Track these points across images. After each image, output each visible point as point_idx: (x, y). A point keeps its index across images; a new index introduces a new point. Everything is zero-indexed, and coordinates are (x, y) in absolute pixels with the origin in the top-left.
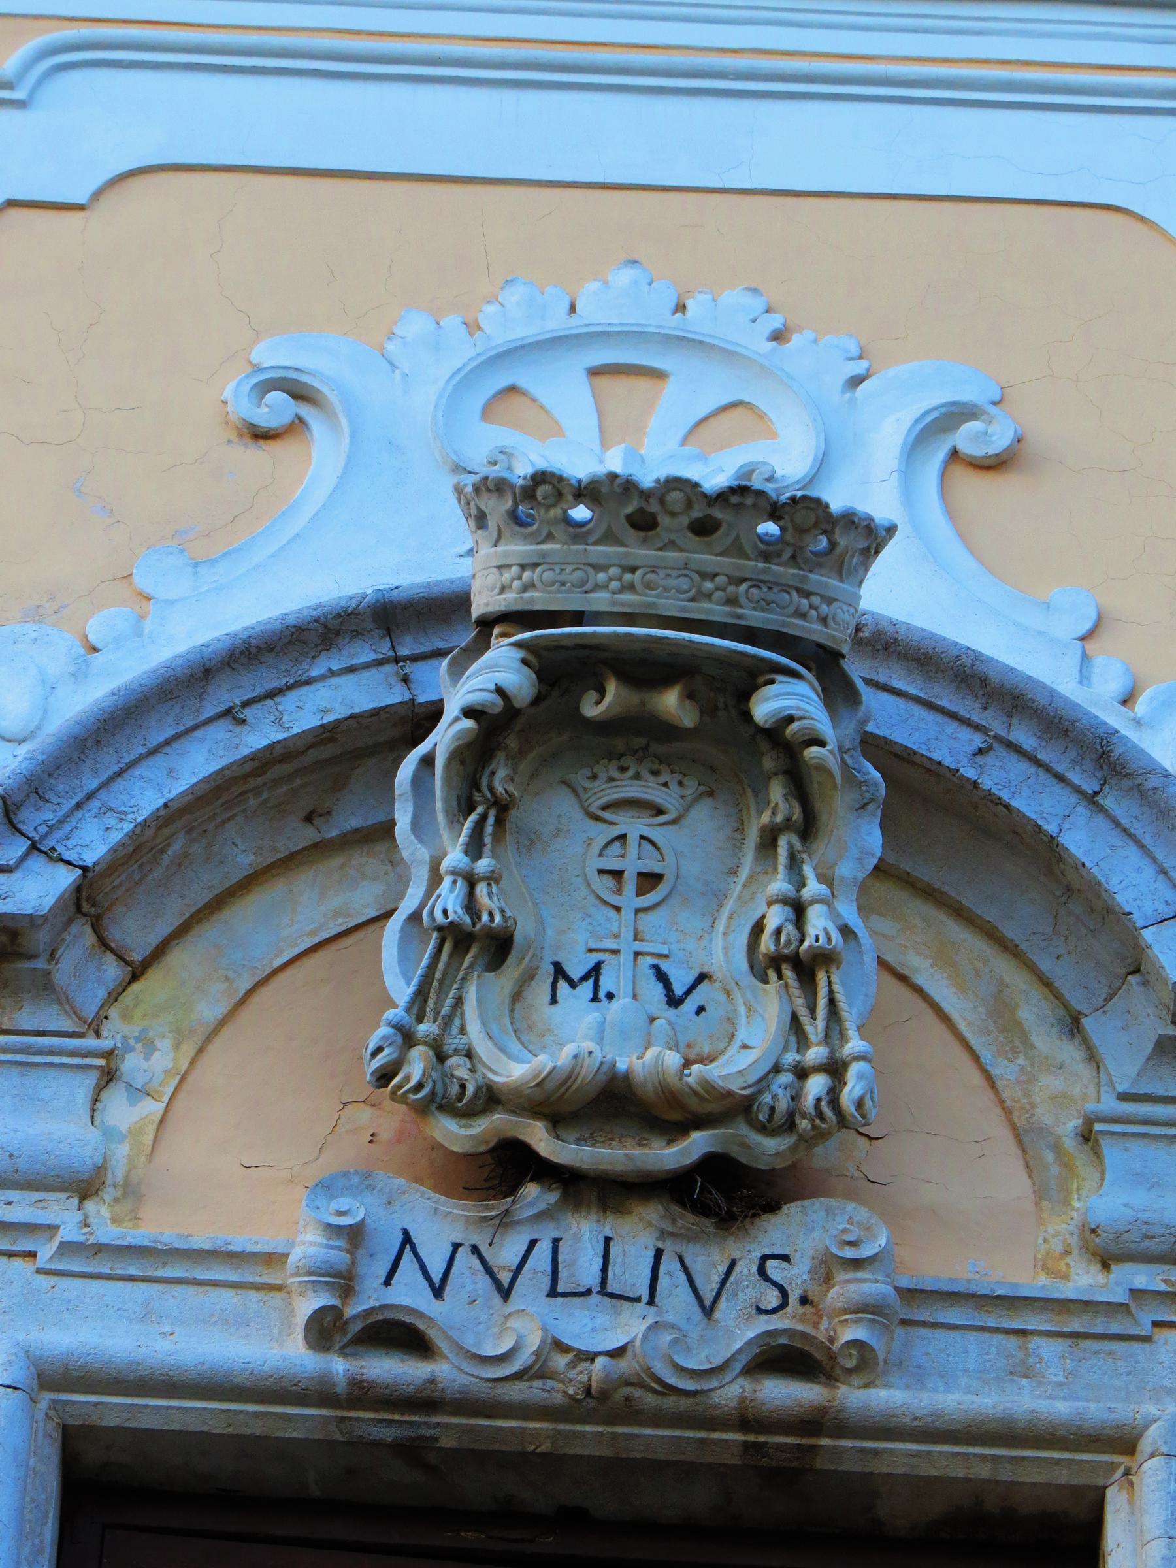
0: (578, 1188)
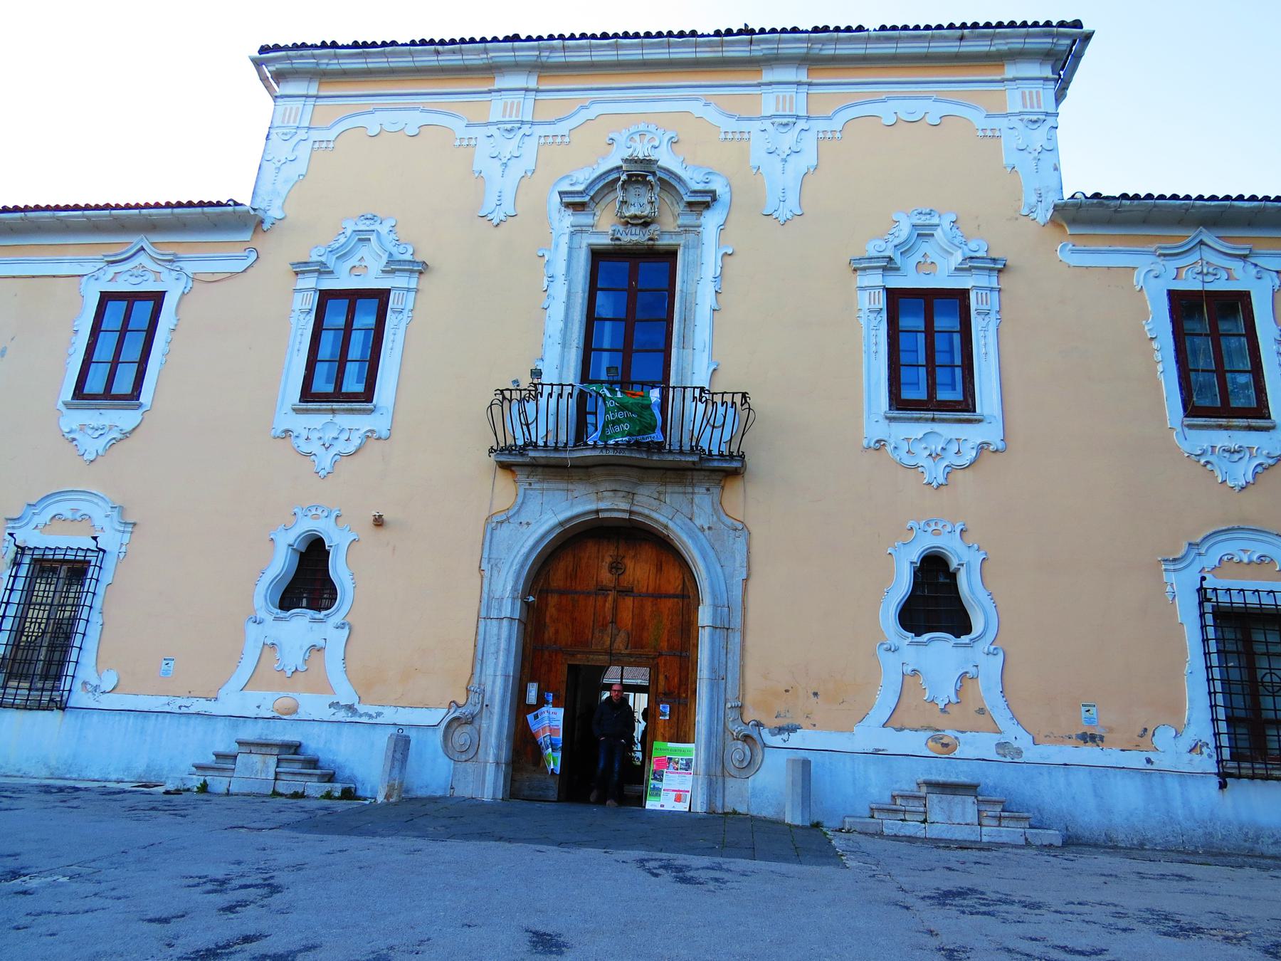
0: (636, 225)
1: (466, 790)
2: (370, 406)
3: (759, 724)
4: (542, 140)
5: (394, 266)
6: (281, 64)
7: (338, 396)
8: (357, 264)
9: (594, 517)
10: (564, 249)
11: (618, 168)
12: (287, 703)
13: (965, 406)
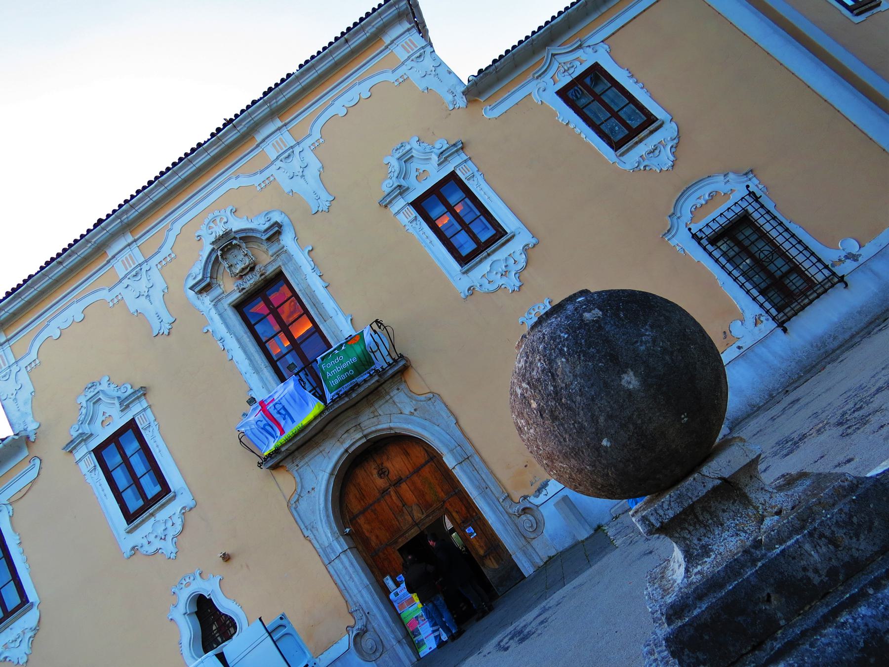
0: (247, 273)
2: (171, 495)
3: (525, 497)
4: (159, 266)
7: (149, 503)
8: (103, 418)
9: (346, 455)
10: (216, 318)
11: (213, 250)
13: (500, 234)
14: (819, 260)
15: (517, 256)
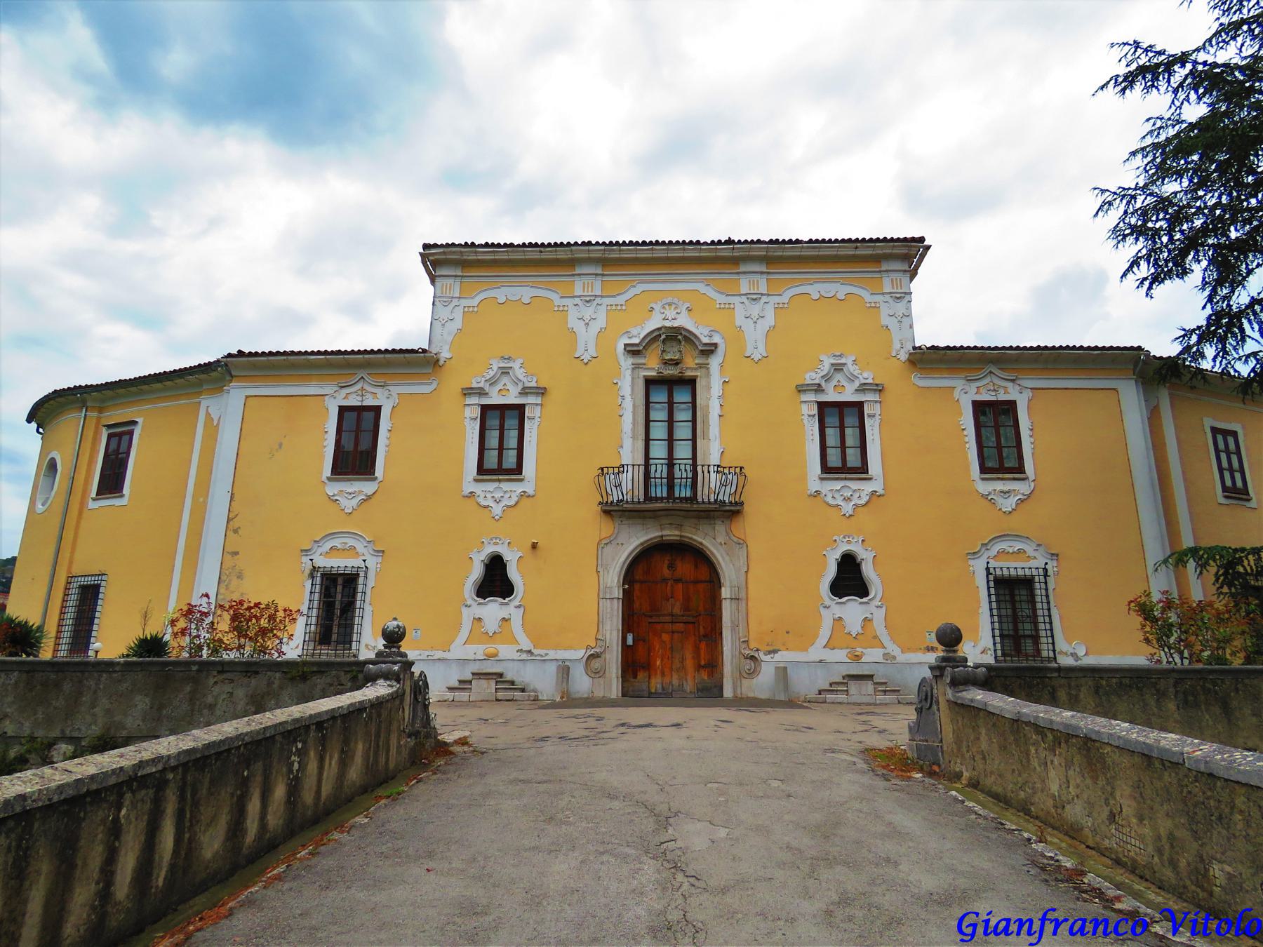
1: (599, 693)
5: (525, 392)
6: (439, 259)
10: (628, 378)
12: (492, 651)
13: (862, 470)
14: (1053, 644)
15: (863, 494)
